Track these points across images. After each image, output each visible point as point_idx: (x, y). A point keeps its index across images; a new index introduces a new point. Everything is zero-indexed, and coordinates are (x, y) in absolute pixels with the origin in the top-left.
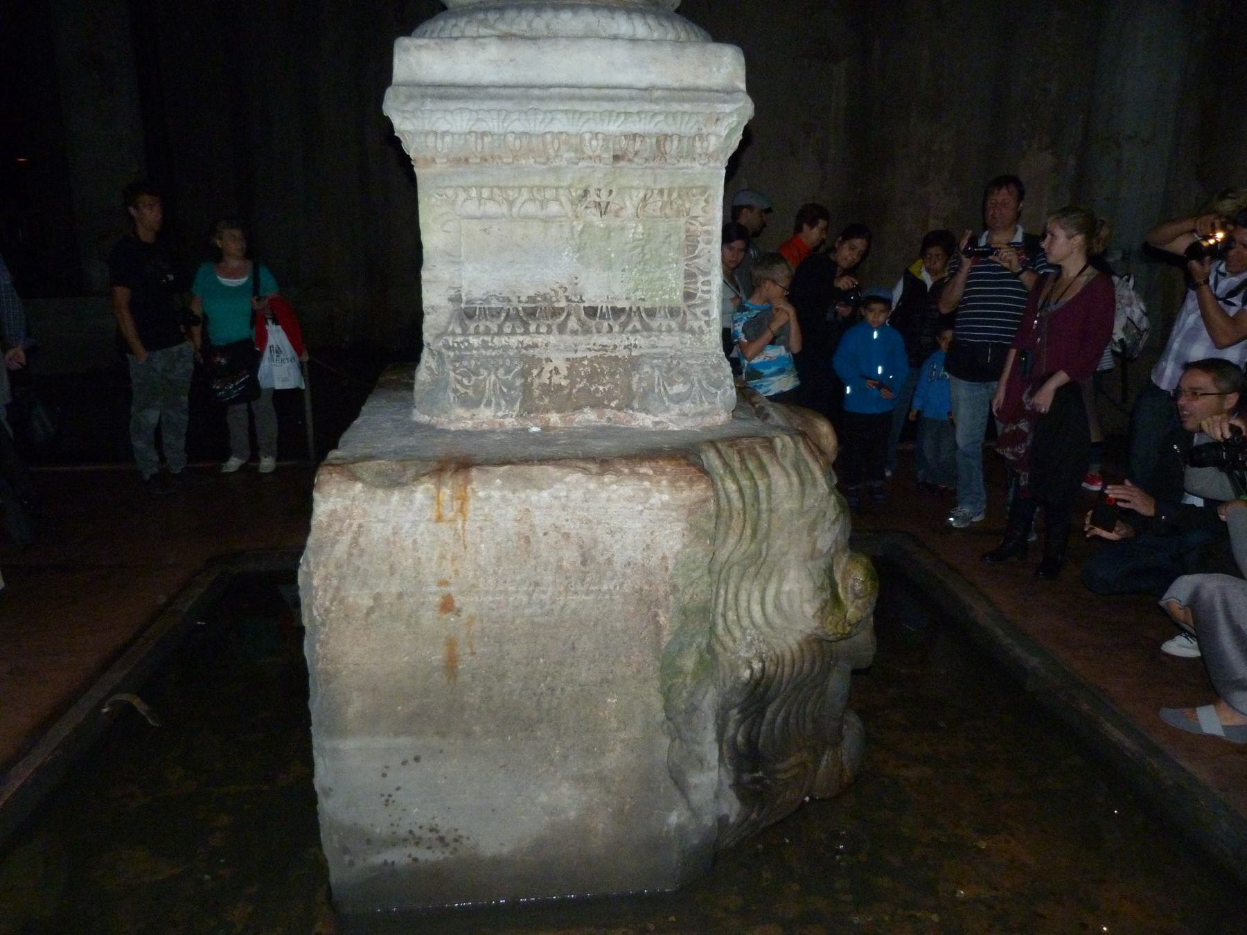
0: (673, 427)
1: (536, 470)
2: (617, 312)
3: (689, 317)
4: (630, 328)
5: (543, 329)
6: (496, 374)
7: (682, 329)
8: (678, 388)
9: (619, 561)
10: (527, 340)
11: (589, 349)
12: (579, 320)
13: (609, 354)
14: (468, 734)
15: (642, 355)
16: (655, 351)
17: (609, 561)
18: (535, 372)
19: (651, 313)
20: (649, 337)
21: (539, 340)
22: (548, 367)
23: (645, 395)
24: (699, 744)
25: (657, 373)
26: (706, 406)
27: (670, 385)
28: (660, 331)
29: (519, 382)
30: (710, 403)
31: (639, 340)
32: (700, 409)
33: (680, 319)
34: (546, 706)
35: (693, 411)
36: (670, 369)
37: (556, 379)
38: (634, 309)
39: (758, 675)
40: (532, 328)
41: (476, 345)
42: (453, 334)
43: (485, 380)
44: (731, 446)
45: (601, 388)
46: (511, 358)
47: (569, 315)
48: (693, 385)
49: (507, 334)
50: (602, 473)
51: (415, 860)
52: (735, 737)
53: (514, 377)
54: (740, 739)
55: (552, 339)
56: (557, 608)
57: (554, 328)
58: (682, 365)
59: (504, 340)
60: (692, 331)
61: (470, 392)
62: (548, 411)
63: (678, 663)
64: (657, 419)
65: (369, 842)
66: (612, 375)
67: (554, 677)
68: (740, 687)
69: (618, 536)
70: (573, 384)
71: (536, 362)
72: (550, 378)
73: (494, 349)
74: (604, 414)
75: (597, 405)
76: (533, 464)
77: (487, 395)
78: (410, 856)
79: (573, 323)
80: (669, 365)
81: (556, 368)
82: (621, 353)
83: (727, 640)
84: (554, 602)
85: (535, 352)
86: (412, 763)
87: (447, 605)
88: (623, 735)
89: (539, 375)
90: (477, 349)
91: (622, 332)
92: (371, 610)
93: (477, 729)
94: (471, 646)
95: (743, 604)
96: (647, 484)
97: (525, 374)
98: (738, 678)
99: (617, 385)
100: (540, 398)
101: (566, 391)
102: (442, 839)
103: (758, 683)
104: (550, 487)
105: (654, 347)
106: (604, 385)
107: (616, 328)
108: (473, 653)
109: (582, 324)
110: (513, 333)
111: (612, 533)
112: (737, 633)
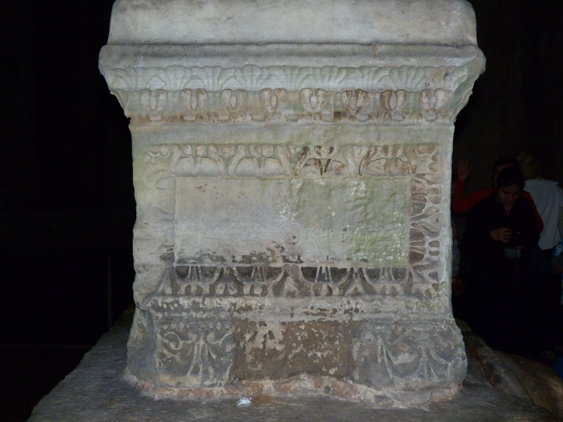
0: (398, 405)
2: (337, 273)
3: (415, 279)
4: (351, 290)
5: (258, 291)
6: (205, 339)
7: (408, 293)
10: (240, 302)
11: (307, 313)
12: (297, 281)
13: (328, 318)
15: (364, 321)
16: (377, 316)
18: (248, 336)
19: (374, 274)
20: (373, 300)
21: (253, 302)
22: (263, 331)
23: (366, 365)
25: (380, 341)
26: (436, 380)
27: (394, 355)
28: (384, 295)
29: (229, 348)
30: (440, 376)
31: (361, 304)
32: (428, 383)
33: (405, 281)
35: (421, 386)
36: (394, 336)
37: (270, 344)
38: (356, 270)
40: (246, 290)
41: (186, 307)
42: (163, 294)
43: (193, 344)
45: (319, 354)
46: (222, 321)
47: (286, 275)
48: (420, 356)
49: (219, 296)
53: (224, 343)
55: (267, 302)
57: (270, 290)
58: (407, 333)
59: (216, 302)
60: (418, 295)
61: (177, 357)
62: (261, 377)
64: (380, 393)
66: (331, 340)
70: (289, 349)
71: (248, 325)
73: (204, 311)
75: (315, 371)
77: (194, 362)
79: (290, 285)
80: (393, 332)
81: (270, 333)
82: (341, 317)
85: (249, 315)
89: (252, 339)
90: (187, 311)
91: (343, 295)
97: (237, 338)
99: (336, 352)
100: (253, 363)
101: (281, 357)
105: (377, 311)
106: (321, 351)
107: (336, 291)
109: (300, 285)
110: (226, 295)
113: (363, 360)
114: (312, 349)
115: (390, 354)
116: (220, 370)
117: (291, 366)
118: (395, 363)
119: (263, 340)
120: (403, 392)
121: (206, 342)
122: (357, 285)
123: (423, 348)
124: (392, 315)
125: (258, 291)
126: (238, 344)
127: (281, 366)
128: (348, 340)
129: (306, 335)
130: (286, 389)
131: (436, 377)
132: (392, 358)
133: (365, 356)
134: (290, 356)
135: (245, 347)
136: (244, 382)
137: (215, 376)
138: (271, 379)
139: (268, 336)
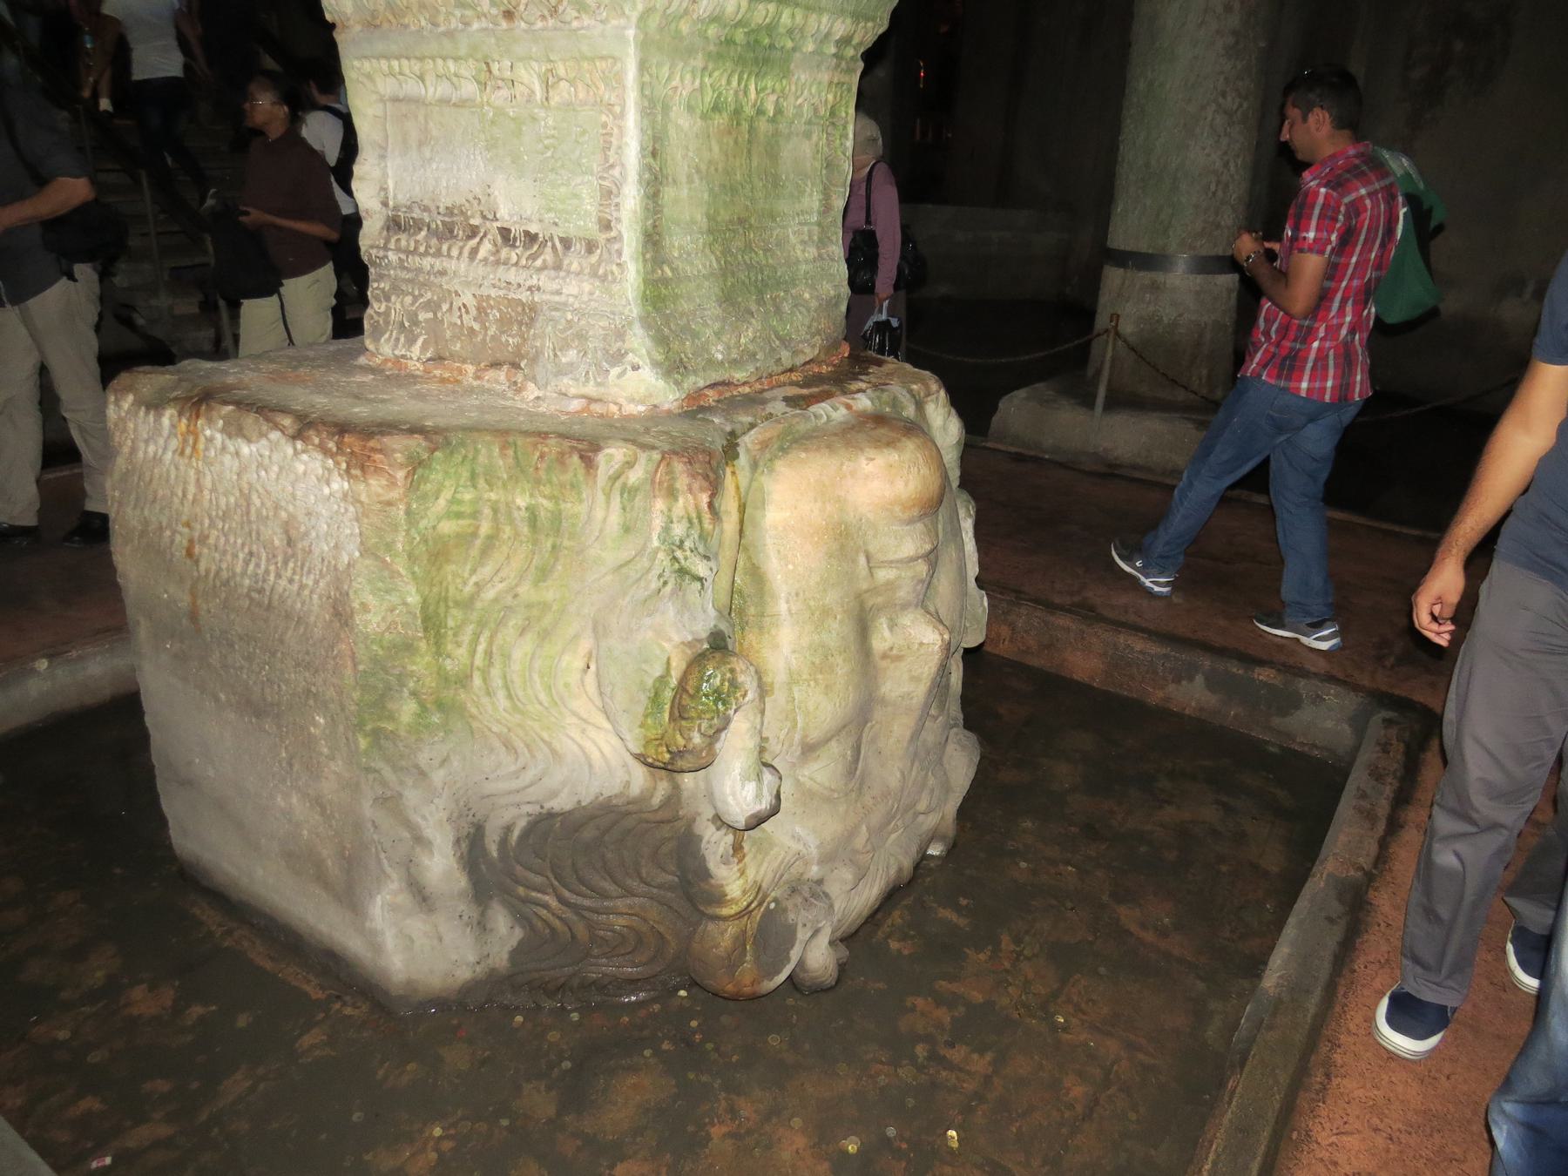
1: (250, 420)
4: (539, 263)
5: (455, 253)
7: (594, 274)
8: (571, 355)
9: (316, 552)
16: (557, 298)
18: (445, 307)
21: (451, 265)
22: (457, 303)
30: (598, 384)
31: (543, 280)
33: (594, 259)
35: (573, 391)
50: (294, 438)
55: (463, 265)
60: (603, 279)
69: (313, 521)
79: (485, 249)
82: (524, 296)
101: (480, 338)
105: (558, 293)
110: (426, 254)
111: (309, 514)
118: (564, 360)
122: (548, 255)
124: (571, 300)
125: (455, 253)
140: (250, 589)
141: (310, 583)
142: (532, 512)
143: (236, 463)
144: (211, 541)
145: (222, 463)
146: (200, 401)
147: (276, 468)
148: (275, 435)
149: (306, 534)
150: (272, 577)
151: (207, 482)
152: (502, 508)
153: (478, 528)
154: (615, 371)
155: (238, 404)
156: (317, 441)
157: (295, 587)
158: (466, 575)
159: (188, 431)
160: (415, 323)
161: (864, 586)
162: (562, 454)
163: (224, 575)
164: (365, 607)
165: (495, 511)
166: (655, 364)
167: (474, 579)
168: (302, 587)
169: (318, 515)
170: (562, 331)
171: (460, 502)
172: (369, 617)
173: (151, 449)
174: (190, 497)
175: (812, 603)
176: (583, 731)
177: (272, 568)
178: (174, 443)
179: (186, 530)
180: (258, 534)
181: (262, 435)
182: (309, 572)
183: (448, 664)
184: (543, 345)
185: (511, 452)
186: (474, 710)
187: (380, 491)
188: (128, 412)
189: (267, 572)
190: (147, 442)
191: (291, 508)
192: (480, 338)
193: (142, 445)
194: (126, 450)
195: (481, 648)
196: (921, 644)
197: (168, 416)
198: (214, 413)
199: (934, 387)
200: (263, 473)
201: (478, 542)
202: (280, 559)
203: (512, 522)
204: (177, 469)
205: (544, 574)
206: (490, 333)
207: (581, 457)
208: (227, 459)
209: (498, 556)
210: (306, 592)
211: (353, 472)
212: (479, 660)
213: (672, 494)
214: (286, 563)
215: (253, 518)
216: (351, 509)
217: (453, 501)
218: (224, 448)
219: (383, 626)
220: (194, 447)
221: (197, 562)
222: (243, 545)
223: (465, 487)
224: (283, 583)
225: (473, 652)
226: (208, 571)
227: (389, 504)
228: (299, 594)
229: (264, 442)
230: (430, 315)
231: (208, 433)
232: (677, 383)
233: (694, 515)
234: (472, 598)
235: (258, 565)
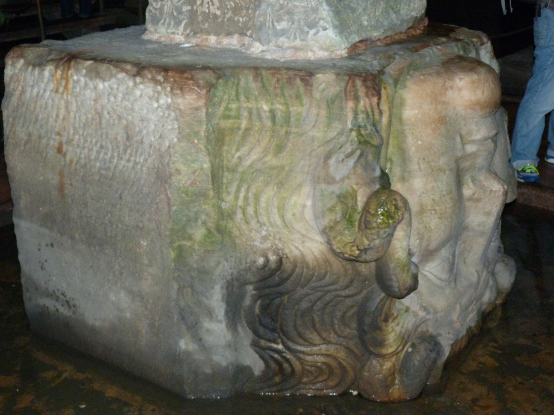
0: (268, 56)
1: (103, 67)
8: (283, 25)
9: (146, 142)
14: (73, 238)
17: (142, 142)
23: (260, 28)
24: (207, 298)
25: (269, 10)
26: (298, 43)
27: (277, 21)
29: (186, 8)
30: (302, 40)
32: (293, 44)
34: (109, 234)
35: (286, 45)
39: (273, 264)
44: (273, 75)
45: (241, 19)
48: (293, 23)
50: (135, 76)
51: (57, 310)
52: (251, 307)
53: (182, 4)
54: (257, 311)
56: (112, 167)
58: (290, 5)
61: (158, 13)
62: (209, 34)
63: (189, 231)
65: (36, 289)
66: (248, 9)
67: (111, 215)
68: (254, 269)
69: (145, 124)
72: (208, 8)
74: (243, 40)
76: (104, 63)
77: (164, 16)
78: (55, 306)
83: (244, 227)
84: (110, 162)
86: (50, 246)
87: (59, 150)
88: (150, 270)
92: (27, 143)
93: (77, 236)
94: (70, 180)
95: (263, 204)
96: (159, 88)
98: (255, 262)
101: (220, 20)
102: (67, 302)
103: (273, 273)
104: (109, 80)
106: (243, 17)
108: (71, 185)
111: (142, 120)
112: (253, 223)
113: (259, 24)
114: (237, 15)
115: (274, 20)
116: (178, 23)
117: (227, 27)
119: (207, 6)
120: (275, 48)
121: (172, 3)
123: (296, 18)
126: (192, 7)
127: (223, 28)
128: (255, 10)
129: (233, 5)
130: (220, 43)
131: (298, 40)
132: (276, 24)
133: (260, 21)
134: (225, 20)
135: (197, 10)
136: (198, 35)
137: (174, 27)
138: (215, 35)
139: (210, 3)
140: (100, 169)
141: (142, 161)
142: (272, 112)
143: (94, 95)
144: (75, 142)
145: (85, 95)
146: (70, 59)
147: (120, 95)
148: (121, 75)
149: (140, 132)
150: (115, 160)
151: (73, 107)
152: (254, 112)
153: (240, 124)
154: (312, 32)
155: (95, 59)
156: (150, 76)
157: (131, 164)
158: (233, 152)
159: (62, 78)
160: (180, 12)
161: (460, 154)
162: (290, 78)
163: (83, 161)
164: (178, 171)
165: (250, 114)
166: (335, 27)
167: (238, 154)
168: (136, 163)
169: (148, 120)
170: (278, 11)
171: (230, 110)
172: (181, 177)
173: (35, 91)
174: (61, 117)
175: (432, 164)
176: (303, 242)
177: (116, 154)
178: (52, 86)
179: (57, 137)
180: (107, 134)
181: (112, 76)
182: (141, 154)
183: (224, 205)
184: (265, 20)
185: (260, 79)
186: (237, 233)
187: (192, 101)
188: (20, 70)
189: (112, 157)
190: (33, 87)
191: (130, 118)
192: (220, 20)
193: (29, 89)
194: (18, 92)
195: (242, 195)
196: (491, 191)
197: (48, 70)
198: (80, 66)
199: (485, 40)
200: (112, 99)
201: (241, 132)
202: (121, 148)
203: (260, 118)
204: (53, 101)
205: (280, 149)
206: (228, 16)
207: (302, 80)
208: (88, 92)
209: (252, 140)
210: (139, 167)
211: (175, 92)
212: (240, 202)
213: (356, 99)
214: (125, 151)
215: (104, 125)
216: (173, 114)
217: (227, 109)
218: (86, 85)
219: (189, 182)
220: (66, 87)
221: (65, 155)
222: (96, 142)
223: (233, 100)
224: (123, 162)
225: (237, 198)
226: (71, 161)
227: (197, 109)
228: (133, 168)
229: (114, 80)
230: (189, 8)
231: (75, 78)
232: (347, 38)
233: (369, 110)
234: (237, 166)
235: (106, 154)
